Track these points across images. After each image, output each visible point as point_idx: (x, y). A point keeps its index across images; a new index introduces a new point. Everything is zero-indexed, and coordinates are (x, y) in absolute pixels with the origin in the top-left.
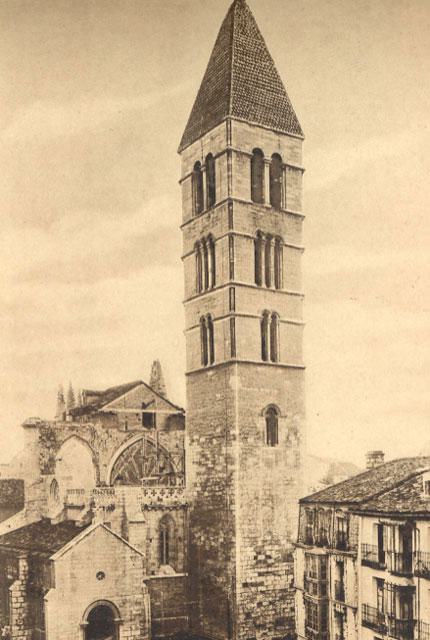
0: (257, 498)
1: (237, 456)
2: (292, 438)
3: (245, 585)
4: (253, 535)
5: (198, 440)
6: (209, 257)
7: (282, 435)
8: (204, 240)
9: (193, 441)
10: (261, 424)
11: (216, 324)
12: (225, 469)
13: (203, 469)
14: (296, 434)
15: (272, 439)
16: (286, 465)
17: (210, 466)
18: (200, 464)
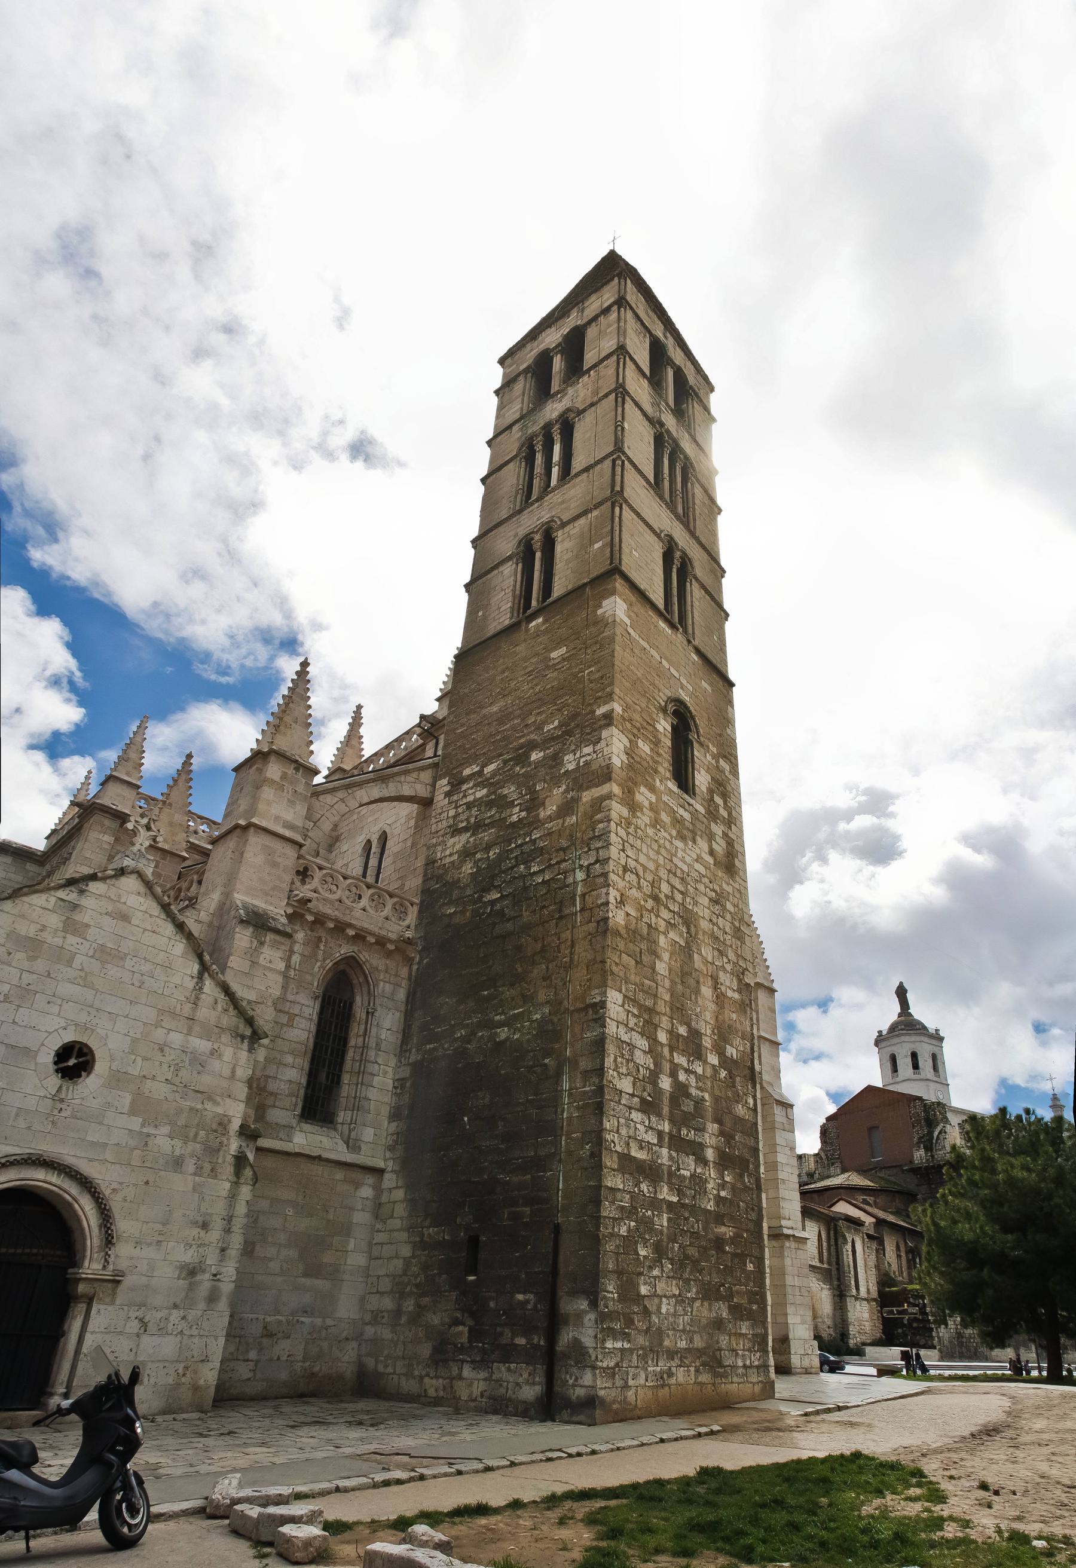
0: (656, 898)
1: (617, 762)
2: (718, 800)
3: (627, 1164)
4: (649, 1003)
5: (480, 773)
6: (557, 448)
7: (702, 780)
8: (547, 427)
9: (457, 784)
10: (664, 726)
11: (559, 535)
12: (567, 808)
13: (486, 836)
14: (725, 796)
15: (682, 776)
16: (712, 852)
17: (516, 815)
18: (476, 828)
